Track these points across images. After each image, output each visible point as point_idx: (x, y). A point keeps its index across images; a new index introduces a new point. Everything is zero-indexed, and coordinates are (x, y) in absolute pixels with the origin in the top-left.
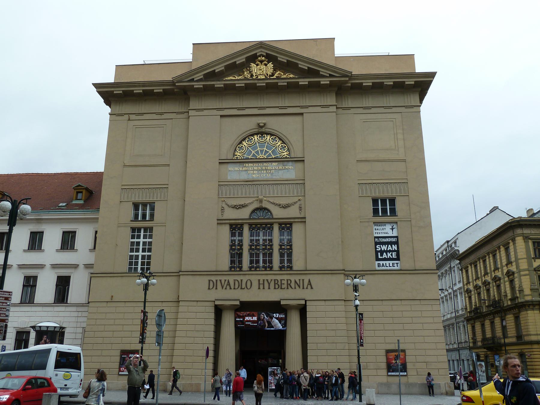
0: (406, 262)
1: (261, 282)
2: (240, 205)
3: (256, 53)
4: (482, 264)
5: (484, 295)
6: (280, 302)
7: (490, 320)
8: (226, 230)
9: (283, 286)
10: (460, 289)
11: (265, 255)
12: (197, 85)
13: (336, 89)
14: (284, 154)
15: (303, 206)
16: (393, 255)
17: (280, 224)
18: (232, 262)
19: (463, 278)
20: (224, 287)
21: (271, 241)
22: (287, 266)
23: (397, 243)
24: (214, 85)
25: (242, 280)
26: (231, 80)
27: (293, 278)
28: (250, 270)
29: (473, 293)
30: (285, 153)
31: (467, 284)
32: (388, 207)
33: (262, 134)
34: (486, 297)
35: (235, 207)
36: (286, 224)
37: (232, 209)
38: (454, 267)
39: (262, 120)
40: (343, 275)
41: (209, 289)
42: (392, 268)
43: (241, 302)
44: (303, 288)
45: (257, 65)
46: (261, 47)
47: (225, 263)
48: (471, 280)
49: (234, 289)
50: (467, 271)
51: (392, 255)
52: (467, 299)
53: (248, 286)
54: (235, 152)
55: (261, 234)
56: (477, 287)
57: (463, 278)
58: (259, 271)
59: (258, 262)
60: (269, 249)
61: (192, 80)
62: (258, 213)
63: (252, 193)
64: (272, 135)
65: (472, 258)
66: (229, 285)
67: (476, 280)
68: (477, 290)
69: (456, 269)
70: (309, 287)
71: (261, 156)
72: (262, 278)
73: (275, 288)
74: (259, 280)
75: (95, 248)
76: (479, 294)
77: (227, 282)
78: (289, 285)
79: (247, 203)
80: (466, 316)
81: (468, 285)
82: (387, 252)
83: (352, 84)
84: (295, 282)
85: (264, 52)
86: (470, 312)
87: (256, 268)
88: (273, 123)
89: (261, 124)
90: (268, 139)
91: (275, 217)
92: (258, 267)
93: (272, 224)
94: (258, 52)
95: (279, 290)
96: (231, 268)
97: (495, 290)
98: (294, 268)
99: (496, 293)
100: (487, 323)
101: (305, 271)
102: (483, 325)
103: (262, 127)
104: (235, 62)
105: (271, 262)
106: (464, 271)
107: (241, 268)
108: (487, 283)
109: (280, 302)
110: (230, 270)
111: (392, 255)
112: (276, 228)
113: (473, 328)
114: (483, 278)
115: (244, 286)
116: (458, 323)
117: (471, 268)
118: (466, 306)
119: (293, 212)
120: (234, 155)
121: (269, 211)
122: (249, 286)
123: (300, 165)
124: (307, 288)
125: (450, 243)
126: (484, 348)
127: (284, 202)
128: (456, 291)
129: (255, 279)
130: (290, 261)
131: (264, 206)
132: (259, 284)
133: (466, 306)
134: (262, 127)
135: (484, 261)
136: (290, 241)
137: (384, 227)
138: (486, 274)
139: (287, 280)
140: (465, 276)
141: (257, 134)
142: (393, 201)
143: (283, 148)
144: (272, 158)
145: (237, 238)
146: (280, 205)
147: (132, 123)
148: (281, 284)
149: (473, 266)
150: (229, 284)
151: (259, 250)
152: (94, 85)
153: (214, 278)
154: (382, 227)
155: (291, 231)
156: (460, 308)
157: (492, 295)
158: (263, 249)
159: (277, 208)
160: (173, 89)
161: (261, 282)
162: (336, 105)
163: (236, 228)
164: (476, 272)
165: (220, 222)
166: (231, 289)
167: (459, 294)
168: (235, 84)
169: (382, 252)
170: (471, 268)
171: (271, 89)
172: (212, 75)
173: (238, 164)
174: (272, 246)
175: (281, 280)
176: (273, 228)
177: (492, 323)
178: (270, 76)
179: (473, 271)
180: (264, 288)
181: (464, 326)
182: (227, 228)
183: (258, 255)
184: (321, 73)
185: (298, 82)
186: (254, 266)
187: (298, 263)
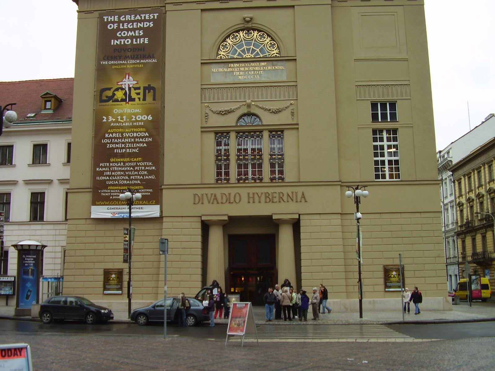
1: (251, 195)
2: (225, 111)
4: (476, 175)
5: (477, 208)
6: (271, 216)
7: (481, 234)
8: (210, 139)
9: (275, 200)
10: (451, 202)
11: (253, 166)
14: (273, 52)
15: (295, 112)
17: (271, 131)
18: (219, 174)
19: (455, 190)
20: (211, 201)
27: (285, 190)
28: (239, 182)
29: (465, 206)
30: (275, 52)
31: (459, 197)
33: (248, 30)
34: (479, 210)
35: (220, 113)
36: (276, 131)
37: (216, 115)
38: (446, 179)
39: (248, 14)
40: (339, 187)
43: (230, 217)
47: (211, 176)
48: (463, 193)
49: (222, 203)
50: (460, 183)
52: (459, 212)
53: (237, 200)
54: (218, 51)
55: (249, 143)
56: (470, 200)
57: (455, 190)
58: (248, 183)
59: (246, 174)
60: (258, 159)
62: (245, 118)
63: (238, 97)
64: (259, 31)
65: (466, 169)
67: (469, 192)
68: (469, 203)
69: (448, 181)
70: (303, 200)
71: (248, 55)
72: (252, 191)
74: (249, 194)
75: (69, 161)
76: (472, 207)
77: (213, 195)
78: (281, 199)
79: (233, 108)
80: (456, 231)
81: (461, 198)
84: (288, 195)
86: (461, 226)
87: (245, 180)
88: (261, 18)
89: (248, 19)
90: (255, 36)
92: (247, 179)
93: (261, 131)
95: (271, 203)
96: (217, 180)
97: (489, 203)
98: (287, 180)
99: (489, 206)
100: (479, 238)
101: (299, 183)
102: (474, 240)
103: (248, 22)
105: (260, 172)
106: (457, 183)
107: (228, 180)
108: (481, 196)
109: (271, 216)
112: (266, 134)
113: (463, 242)
114: (477, 190)
115: (232, 200)
116: (448, 238)
117: (465, 179)
118: (457, 220)
120: (218, 54)
121: (257, 116)
122: (237, 200)
123: (291, 65)
125: (442, 154)
126: (474, 263)
127: (274, 106)
128: (447, 204)
129: (244, 192)
130: (281, 172)
131: (252, 111)
132: (249, 197)
133: (457, 220)
134: (248, 22)
135: (479, 172)
136: (281, 149)
138: (480, 186)
139: (279, 193)
140: (457, 188)
141: (243, 30)
143: (272, 45)
144: (260, 57)
145: (223, 148)
146: (270, 110)
148: (273, 197)
149: (466, 177)
150: (216, 198)
151: (247, 160)
153: (199, 192)
155: (282, 138)
156: (450, 222)
157: (485, 208)
158: (252, 160)
161: (251, 195)
163: (221, 135)
164: (470, 184)
165: (204, 130)
167: (449, 208)
170: (465, 179)
173: (222, 65)
174: (261, 156)
176: (262, 136)
177: (484, 237)
179: (467, 183)
180: (254, 202)
181: (454, 241)
182: (212, 135)
183: (246, 166)
186: (242, 178)
187: (290, 175)
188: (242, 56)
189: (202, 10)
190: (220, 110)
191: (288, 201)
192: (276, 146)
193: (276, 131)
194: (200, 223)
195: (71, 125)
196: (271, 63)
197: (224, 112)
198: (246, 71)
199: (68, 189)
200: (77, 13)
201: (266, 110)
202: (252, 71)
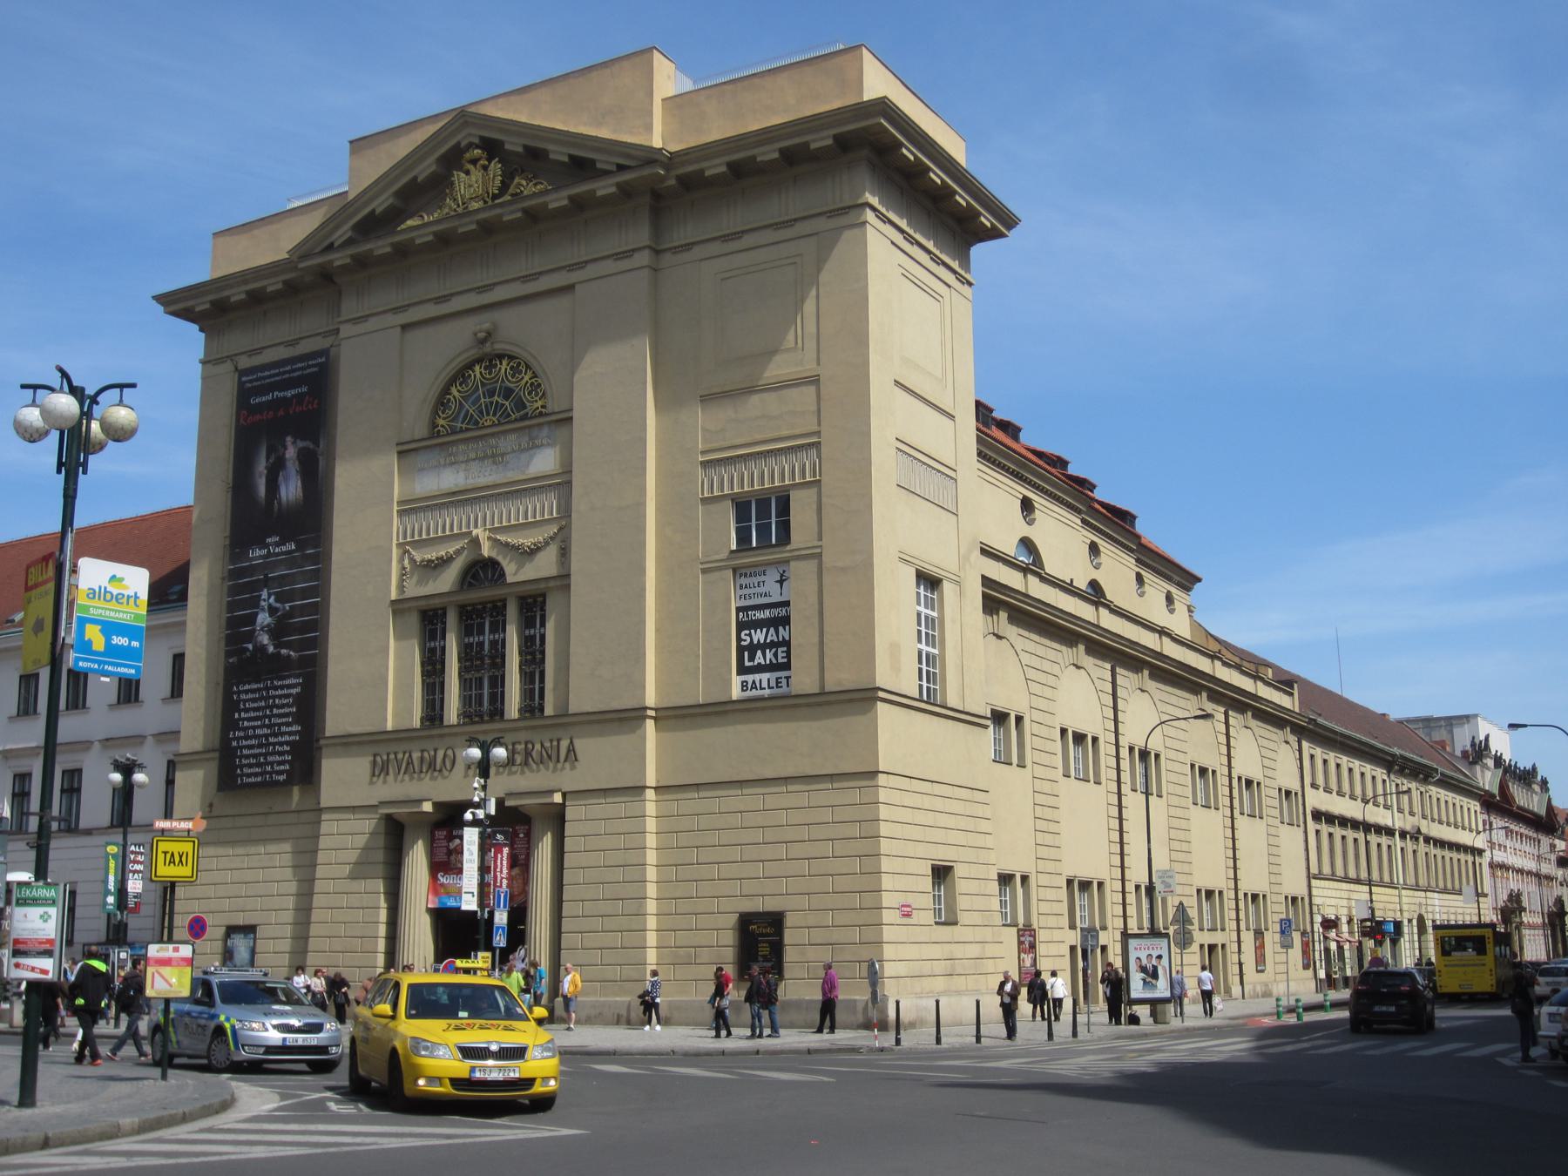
0: (803, 679)
12: (340, 259)
16: (780, 655)
23: (785, 621)
24: (371, 250)
26: (412, 228)
32: (774, 520)
42: (776, 691)
45: (467, 173)
46: (466, 124)
51: (776, 655)
61: (330, 247)
82: (763, 647)
83: (679, 178)
94: (462, 138)
103: (483, 342)
104: (415, 178)
105: (498, 698)
111: (776, 655)
134: (483, 342)
137: (762, 578)
141: (479, 361)
152: (159, 299)
154: (755, 580)
162: (649, 247)
168: (413, 239)
169: (753, 649)
172: (371, 225)
178: (495, 197)
183: (481, 687)
184: (599, 166)
186: (470, 714)
188: (477, 423)
189: (405, 327)
193: (534, 597)
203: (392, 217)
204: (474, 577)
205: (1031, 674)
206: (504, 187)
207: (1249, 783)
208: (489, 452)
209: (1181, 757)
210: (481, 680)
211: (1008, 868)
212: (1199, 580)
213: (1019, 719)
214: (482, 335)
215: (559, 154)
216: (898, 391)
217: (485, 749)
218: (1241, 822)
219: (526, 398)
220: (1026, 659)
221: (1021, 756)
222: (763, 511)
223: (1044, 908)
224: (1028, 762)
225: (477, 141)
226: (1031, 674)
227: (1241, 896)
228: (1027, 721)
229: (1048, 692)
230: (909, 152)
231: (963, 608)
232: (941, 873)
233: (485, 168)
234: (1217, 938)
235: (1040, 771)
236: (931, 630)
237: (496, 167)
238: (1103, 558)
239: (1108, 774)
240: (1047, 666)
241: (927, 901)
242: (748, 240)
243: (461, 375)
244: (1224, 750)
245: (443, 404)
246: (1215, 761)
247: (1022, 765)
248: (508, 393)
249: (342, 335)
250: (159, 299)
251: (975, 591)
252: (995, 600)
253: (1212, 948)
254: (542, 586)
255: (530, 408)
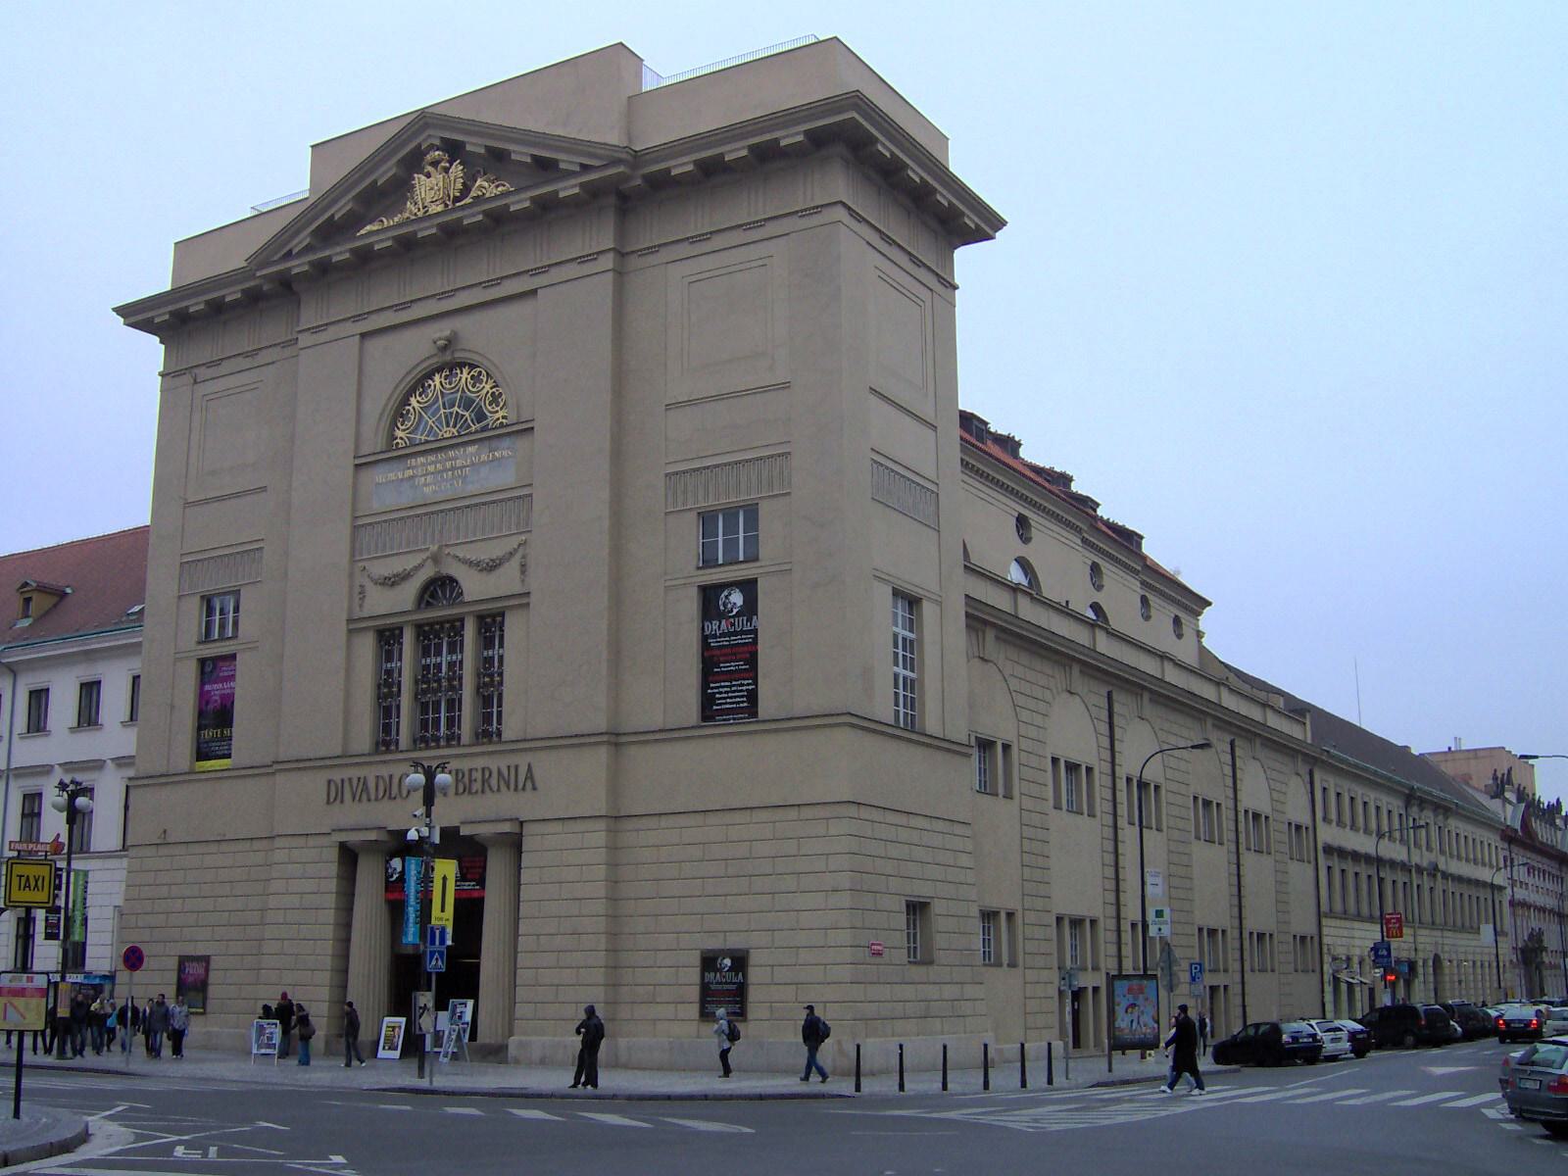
2: (394, 576)
3: (420, 145)
6: (457, 829)
8: (367, 645)
12: (299, 266)
13: (612, 200)
20: (357, 798)
21: (461, 662)
22: (488, 732)
25: (391, 777)
32: (741, 535)
41: (328, 802)
44: (516, 789)
45: (428, 176)
46: (426, 126)
49: (376, 799)
61: (289, 255)
66: (368, 794)
70: (529, 785)
73: (457, 794)
79: (409, 567)
83: (647, 178)
85: (435, 136)
91: (467, 598)
94: (422, 140)
104: (375, 182)
109: (457, 829)
110: (376, 751)
119: (504, 582)
123: (522, 443)
124: (524, 789)
134: (444, 349)
136: (501, 658)
141: (439, 370)
142: (752, 512)
143: (495, 399)
146: (478, 564)
147: (201, 389)
152: (119, 310)
153: (337, 775)
159: (473, 572)
160: (261, 286)
166: (369, 800)
168: (371, 245)
171: (450, 238)
172: (330, 232)
175: (471, 770)
178: (456, 199)
184: (562, 166)
185: (507, 206)
186: (425, 737)
187: (511, 728)
188: (436, 434)
189: (364, 336)
190: (386, 575)
191: (499, 790)
192: (495, 653)
193: (493, 616)
194: (337, 849)
195: (141, 636)
196: (487, 443)
197: (393, 580)
198: (439, 472)
199: (130, 779)
200: (160, 378)
201: (470, 563)
202: (450, 470)
203: (354, 221)
204: (432, 596)
205: (1021, 700)
206: (466, 190)
207: (1256, 816)
208: (448, 465)
209: (1183, 789)
210: (438, 703)
211: (993, 902)
212: (1210, 604)
213: (1006, 747)
214: (441, 343)
215: (521, 154)
216: (874, 400)
217: (430, 775)
218: (1249, 859)
219: (488, 409)
220: (1014, 684)
221: (1008, 786)
222: (731, 528)
223: (1031, 947)
224: (1016, 792)
225: (437, 142)
226: (1021, 700)
227: (1246, 935)
228: (1015, 750)
229: (1038, 720)
230: (885, 148)
231: (944, 633)
232: (917, 909)
233: (446, 170)
234: (1219, 980)
235: (1028, 803)
236: (909, 651)
237: (457, 169)
238: (1106, 581)
239: (1102, 806)
240: (1038, 692)
241: (900, 939)
242: (718, 242)
243: (419, 384)
244: (1229, 782)
245: (402, 415)
246: (1219, 794)
247: (1008, 796)
248: (467, 403)
249: (301, 344)
250: (119, 310)
251: (959, 609)
252: (979, 618)
253: (1213, 989)
254: (499, 604)
255: (489, 421)
